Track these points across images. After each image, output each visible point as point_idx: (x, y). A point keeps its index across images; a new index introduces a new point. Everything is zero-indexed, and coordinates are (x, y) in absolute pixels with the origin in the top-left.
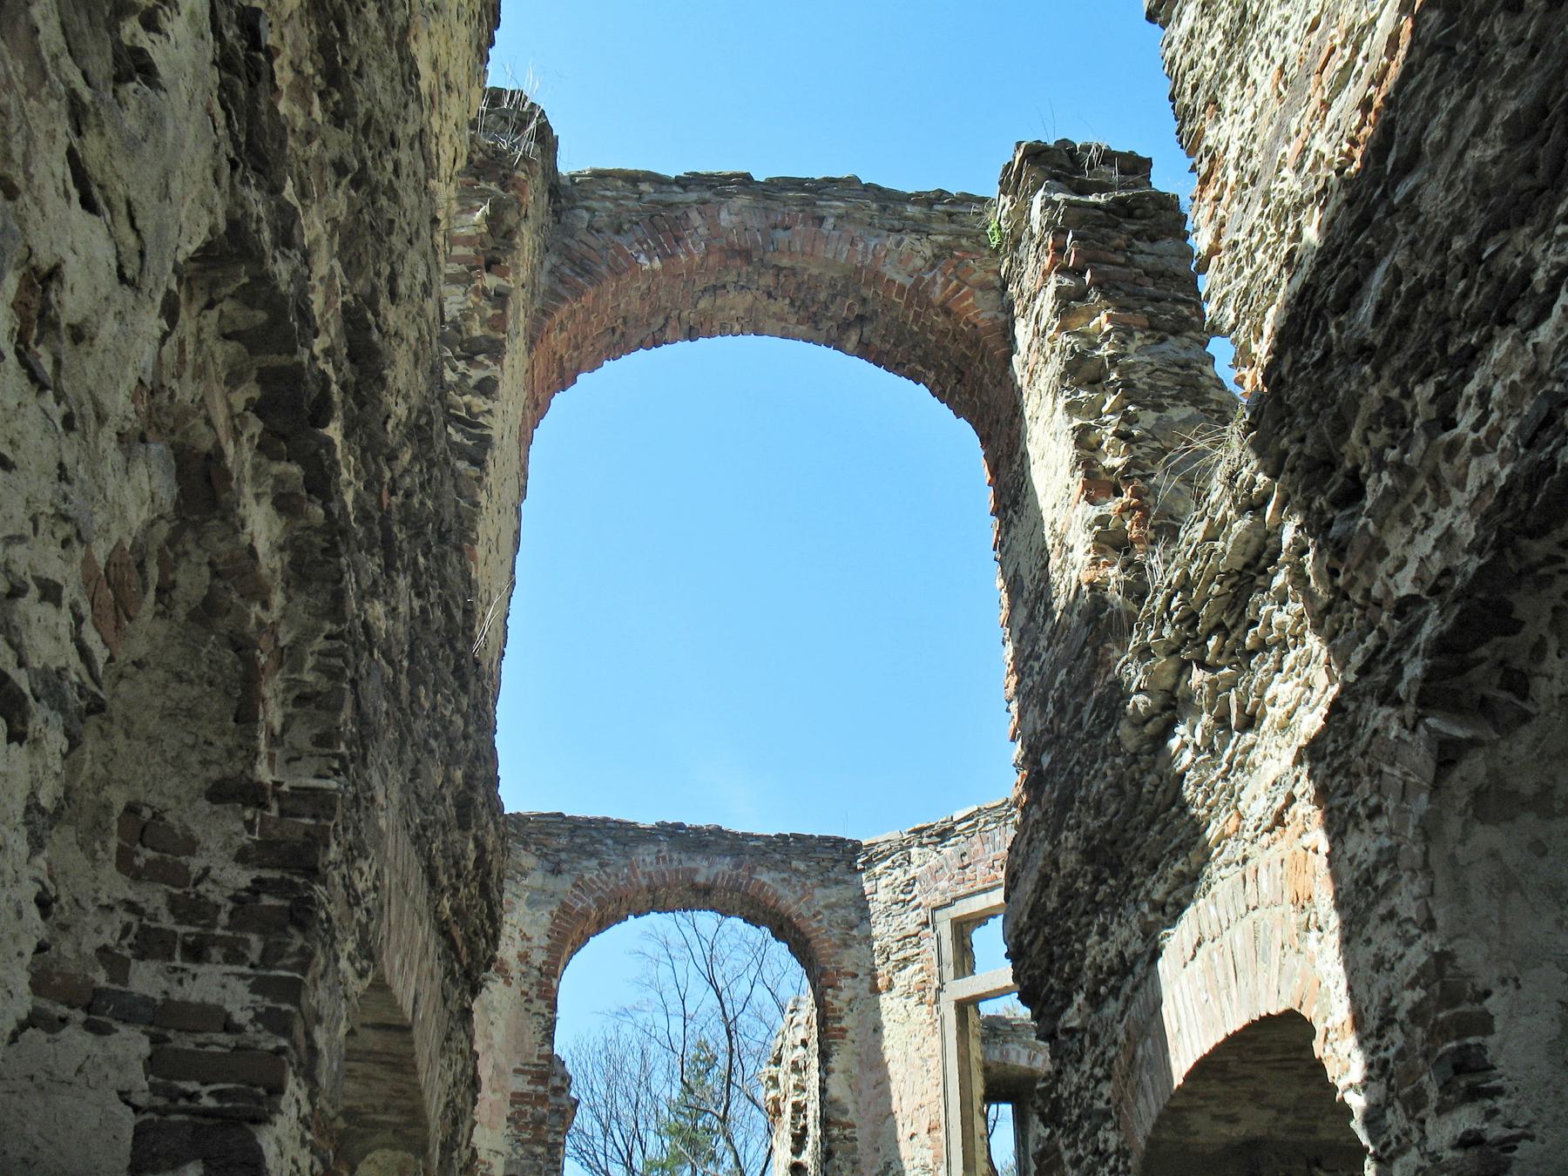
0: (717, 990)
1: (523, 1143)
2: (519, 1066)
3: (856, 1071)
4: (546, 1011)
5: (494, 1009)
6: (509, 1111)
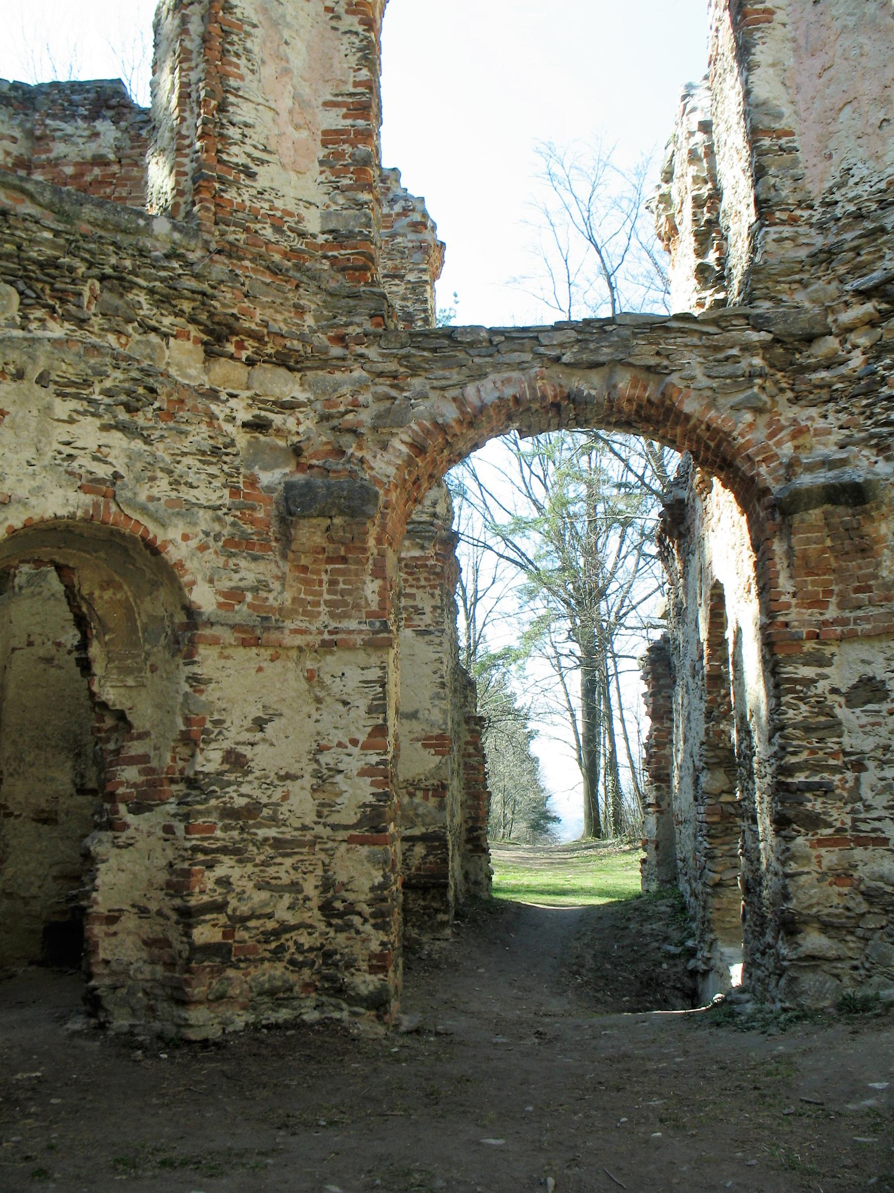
0: (596, 246)
1: (343, 190)
2: (330, 98)
3: (790, 62)
4: (360, 29)
5: (288, 25)
6: (321, 153)
